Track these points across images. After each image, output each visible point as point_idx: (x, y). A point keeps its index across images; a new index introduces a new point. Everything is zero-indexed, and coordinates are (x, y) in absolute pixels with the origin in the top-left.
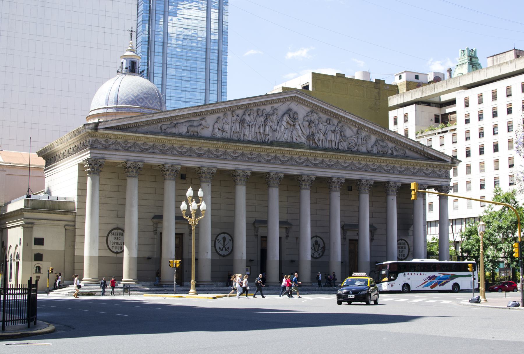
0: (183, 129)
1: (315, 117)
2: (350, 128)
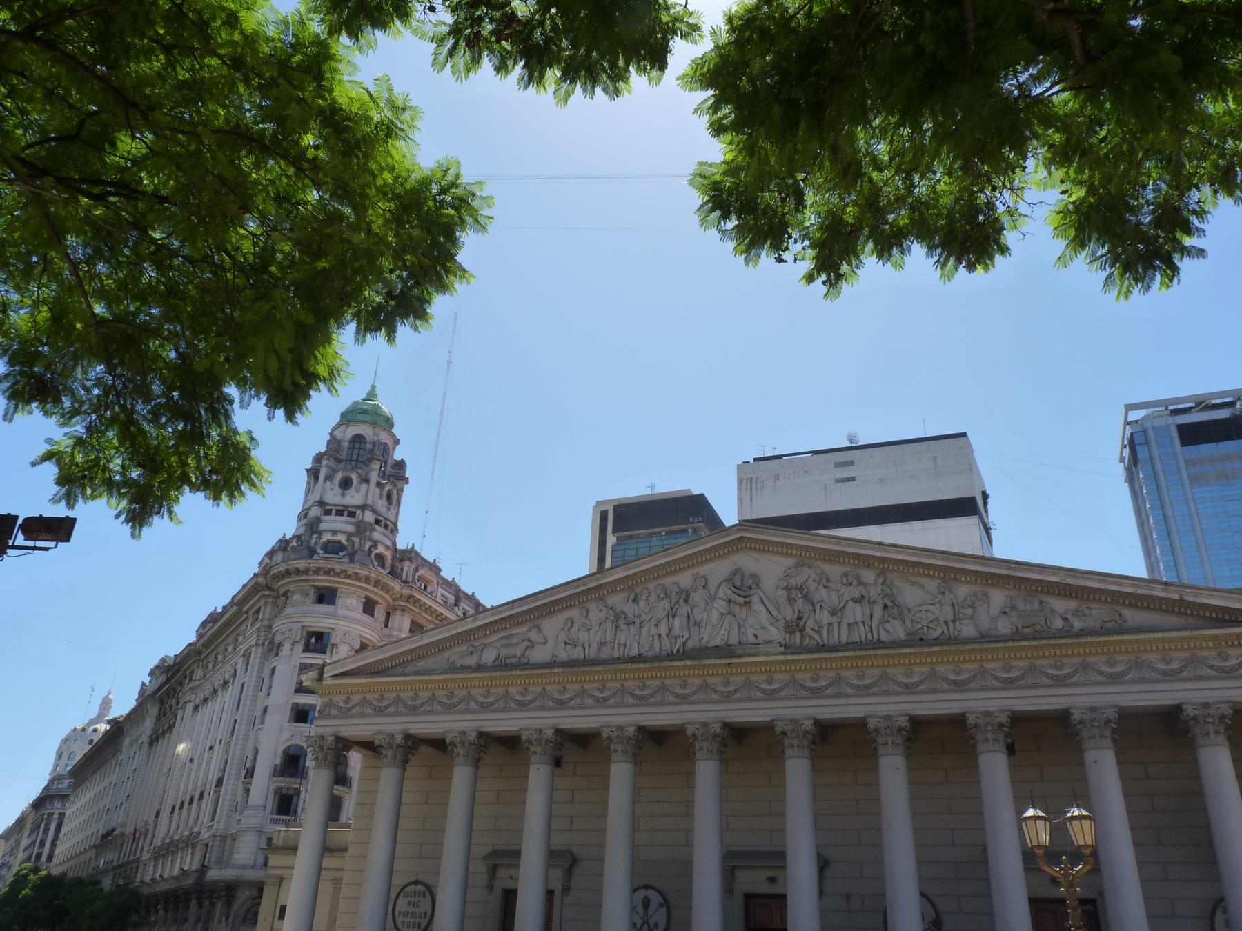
0: (489, 657)
1: (805, 576)
2: (913, 583)
